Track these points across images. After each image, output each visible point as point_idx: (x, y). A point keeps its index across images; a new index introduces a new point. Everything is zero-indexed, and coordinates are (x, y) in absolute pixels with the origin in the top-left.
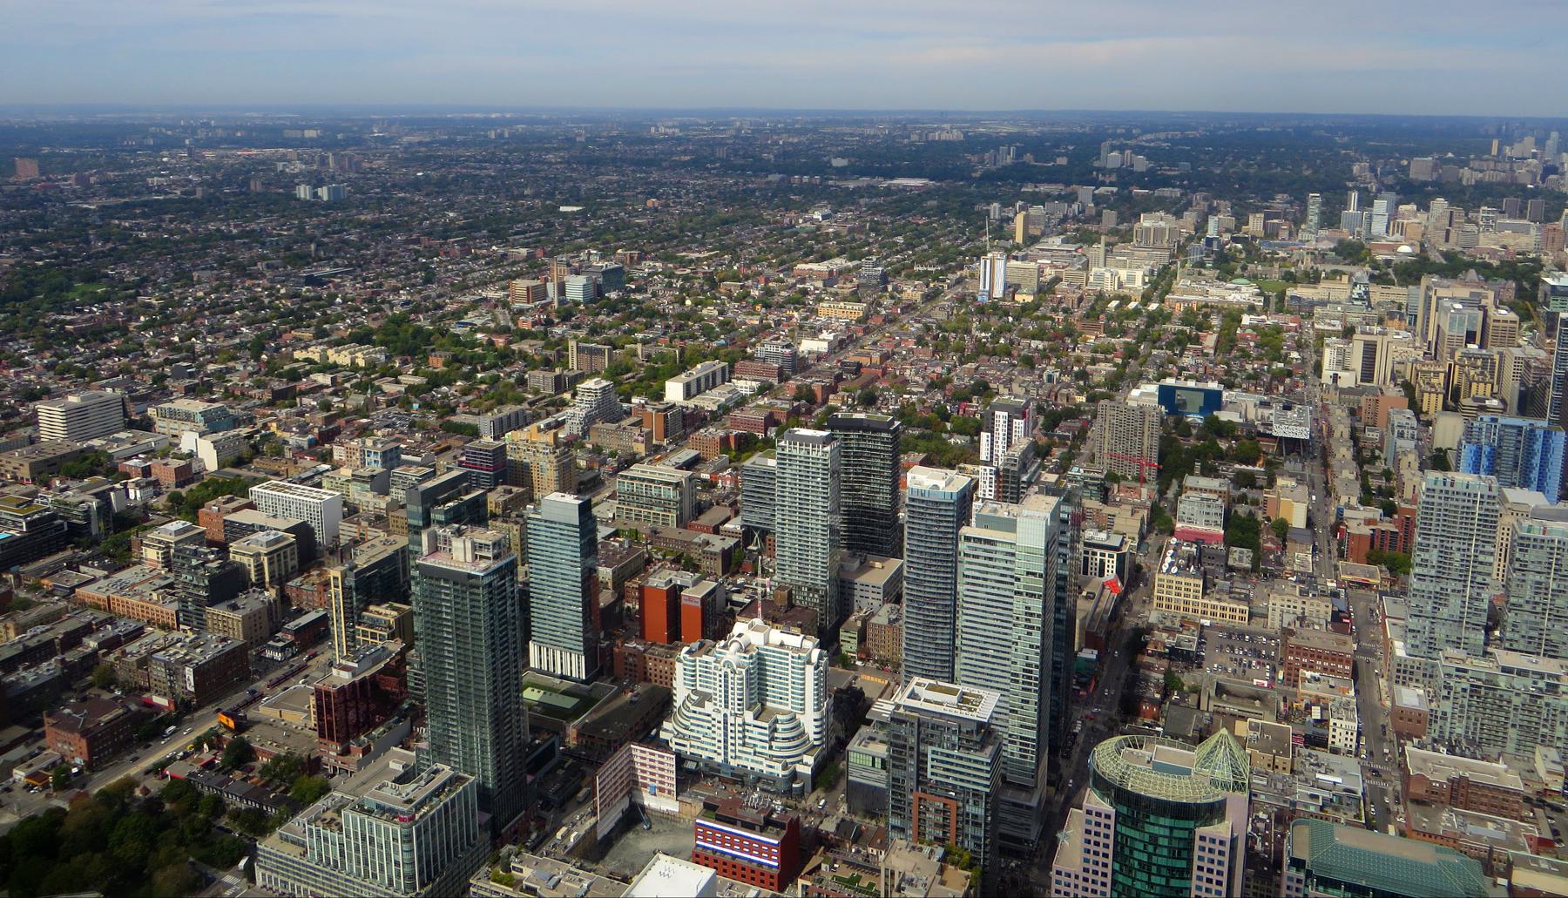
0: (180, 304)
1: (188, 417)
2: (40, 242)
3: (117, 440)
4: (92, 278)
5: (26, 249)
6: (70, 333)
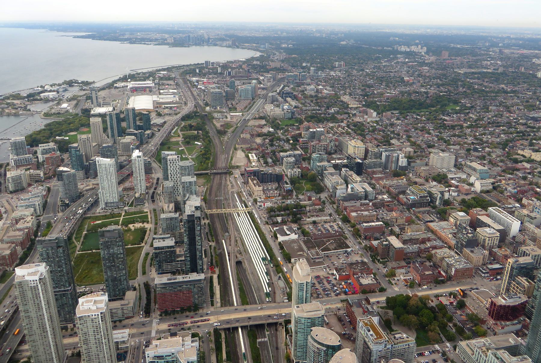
0: (482, 119)
1: (475, 170)
2: (442, 85)
3: (451, 171)
4: (456, 103)
5: (438, 87)
6: (444, 124)
